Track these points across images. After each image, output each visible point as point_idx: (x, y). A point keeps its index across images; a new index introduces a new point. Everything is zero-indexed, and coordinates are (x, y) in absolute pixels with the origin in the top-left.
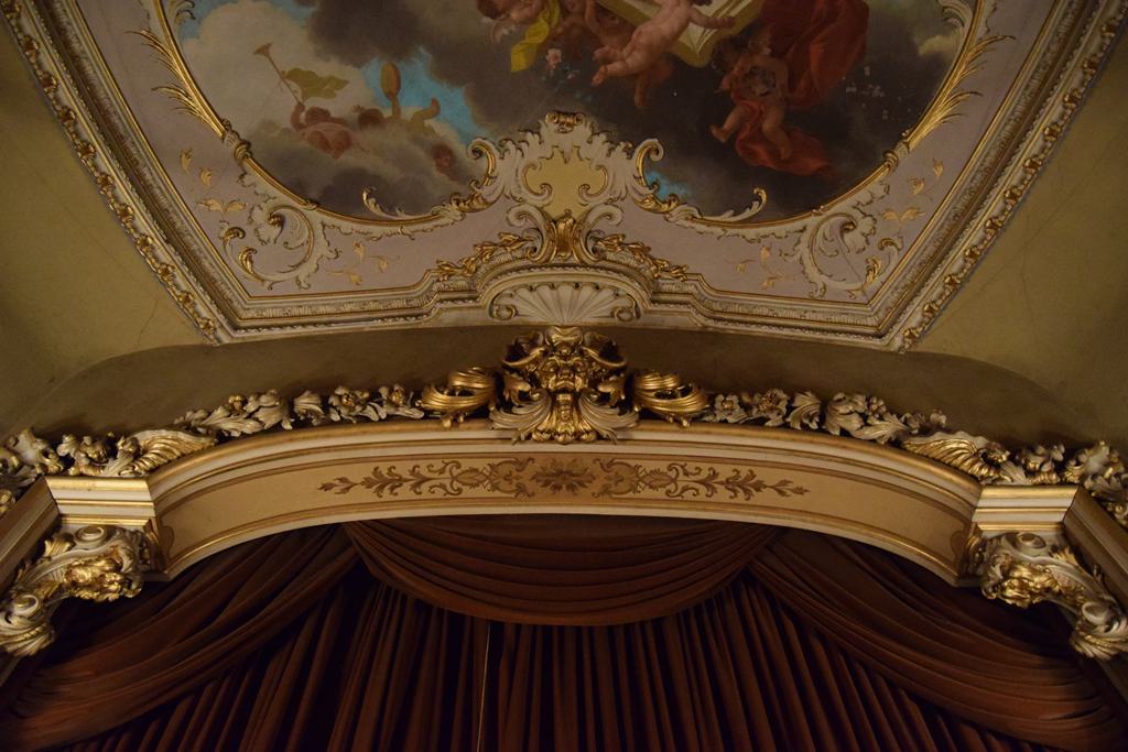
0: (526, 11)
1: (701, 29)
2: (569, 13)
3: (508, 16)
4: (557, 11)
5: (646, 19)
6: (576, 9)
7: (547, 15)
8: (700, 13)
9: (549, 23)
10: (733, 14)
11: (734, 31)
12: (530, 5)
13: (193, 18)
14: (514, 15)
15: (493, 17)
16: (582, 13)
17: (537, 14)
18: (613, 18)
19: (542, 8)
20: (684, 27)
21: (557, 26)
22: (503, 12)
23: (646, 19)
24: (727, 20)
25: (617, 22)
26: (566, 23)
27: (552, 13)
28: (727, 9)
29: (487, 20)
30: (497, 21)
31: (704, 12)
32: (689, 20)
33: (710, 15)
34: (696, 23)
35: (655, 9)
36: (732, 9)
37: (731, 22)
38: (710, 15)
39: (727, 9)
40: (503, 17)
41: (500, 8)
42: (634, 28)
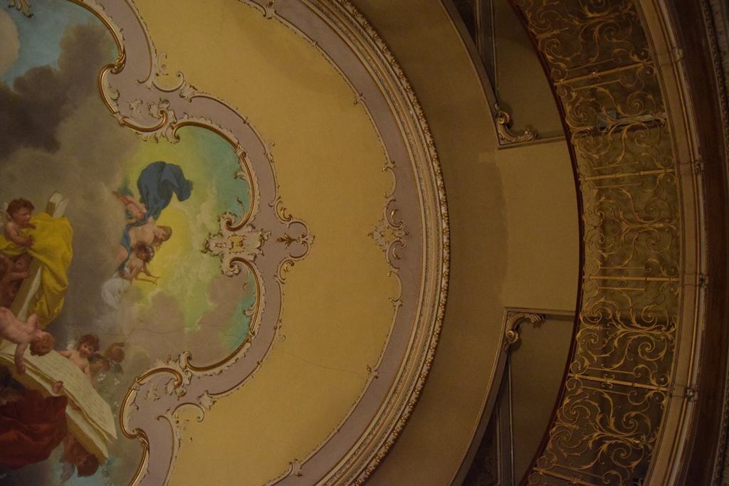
0: (13, 233)
1: (13, 353)
2: (15, 261)
3: (10, 221)
4: (16, 253)
5: (16, 315)
6: (18, 266)
7: (12, 247)
8: (24, 350)
9: (6, 249)
10: (28, 372)
11: (15, 375)
12: (19, 235)
13: (10, 7)
14: (11, 225)
15: (8, 211)
16: (16, 270)
17: (12, 240)
18: (14, 292)
19: (17, 244)
20: (13, 341)
21: (4, 254)
22: (13, 218)
23: (16, 315)
24: (23, 368)
25: (11, 295)
26: (7, 260)
27: (13, 250)
28: (30, 367)
29: (6, 206)
30: (5, 212)
31: (26, 351)
32: (19, 343)
33: (24, 356)
34: (18, 347)
35: (24, 318)
36: (30, 370)
37: (21, 370)
38: (24, 356)
39: (30, 367)
40: (10, 217)
41: (15, 215)
42: (8, 306)
